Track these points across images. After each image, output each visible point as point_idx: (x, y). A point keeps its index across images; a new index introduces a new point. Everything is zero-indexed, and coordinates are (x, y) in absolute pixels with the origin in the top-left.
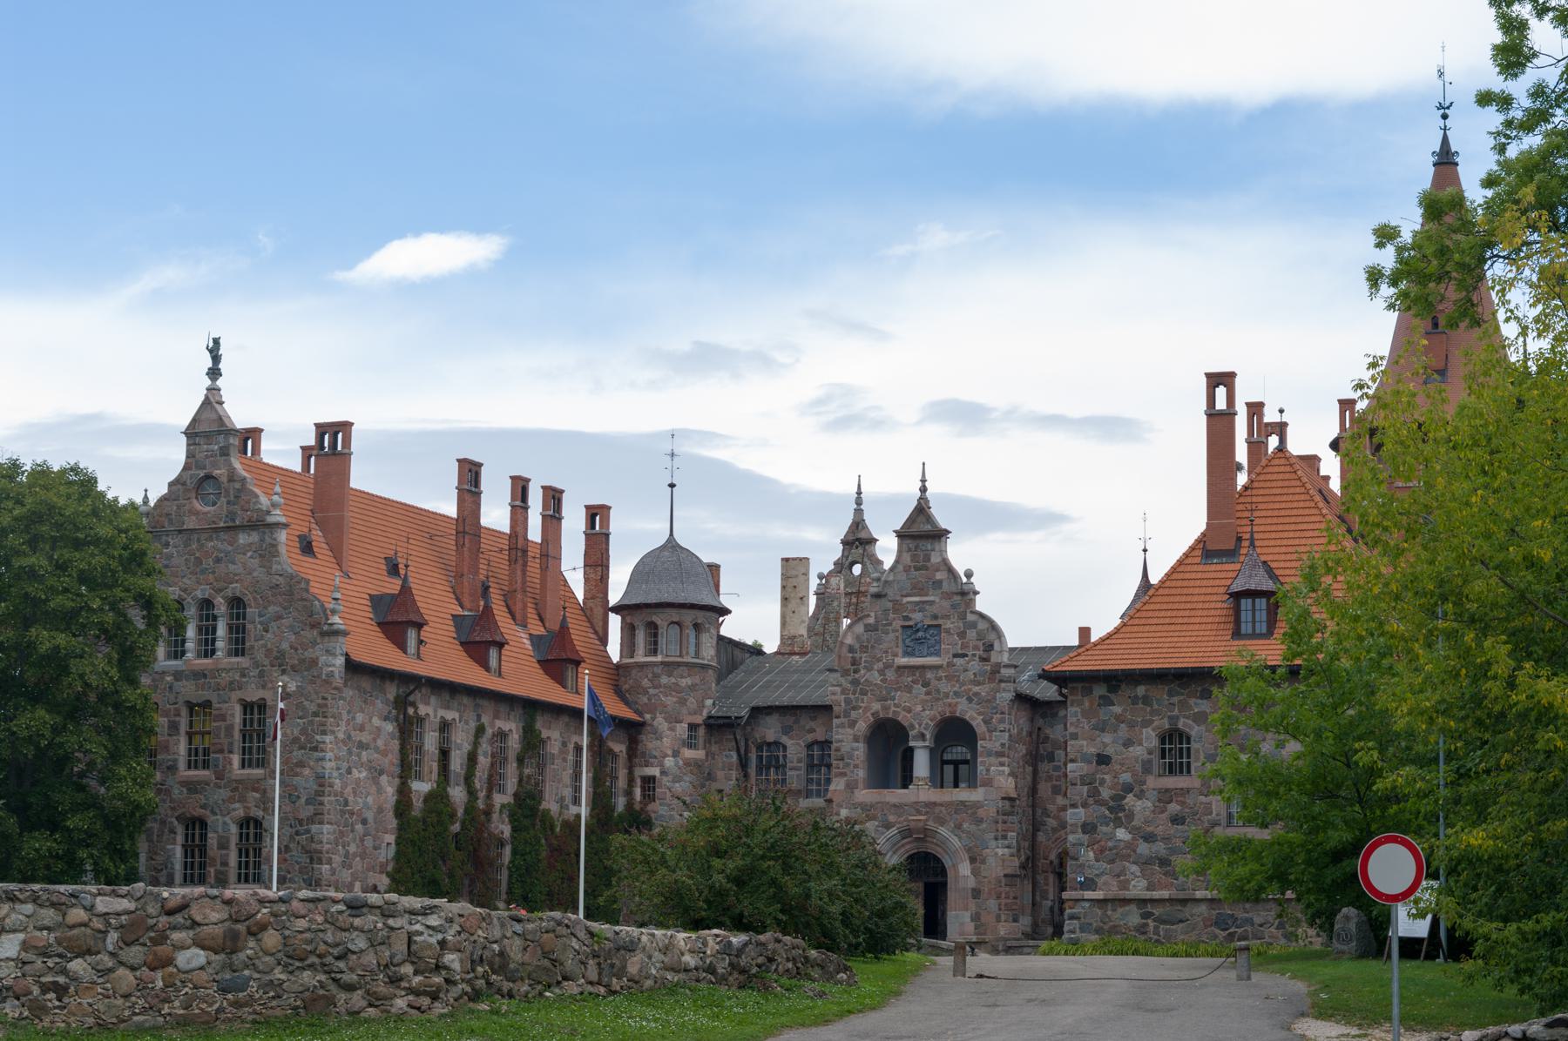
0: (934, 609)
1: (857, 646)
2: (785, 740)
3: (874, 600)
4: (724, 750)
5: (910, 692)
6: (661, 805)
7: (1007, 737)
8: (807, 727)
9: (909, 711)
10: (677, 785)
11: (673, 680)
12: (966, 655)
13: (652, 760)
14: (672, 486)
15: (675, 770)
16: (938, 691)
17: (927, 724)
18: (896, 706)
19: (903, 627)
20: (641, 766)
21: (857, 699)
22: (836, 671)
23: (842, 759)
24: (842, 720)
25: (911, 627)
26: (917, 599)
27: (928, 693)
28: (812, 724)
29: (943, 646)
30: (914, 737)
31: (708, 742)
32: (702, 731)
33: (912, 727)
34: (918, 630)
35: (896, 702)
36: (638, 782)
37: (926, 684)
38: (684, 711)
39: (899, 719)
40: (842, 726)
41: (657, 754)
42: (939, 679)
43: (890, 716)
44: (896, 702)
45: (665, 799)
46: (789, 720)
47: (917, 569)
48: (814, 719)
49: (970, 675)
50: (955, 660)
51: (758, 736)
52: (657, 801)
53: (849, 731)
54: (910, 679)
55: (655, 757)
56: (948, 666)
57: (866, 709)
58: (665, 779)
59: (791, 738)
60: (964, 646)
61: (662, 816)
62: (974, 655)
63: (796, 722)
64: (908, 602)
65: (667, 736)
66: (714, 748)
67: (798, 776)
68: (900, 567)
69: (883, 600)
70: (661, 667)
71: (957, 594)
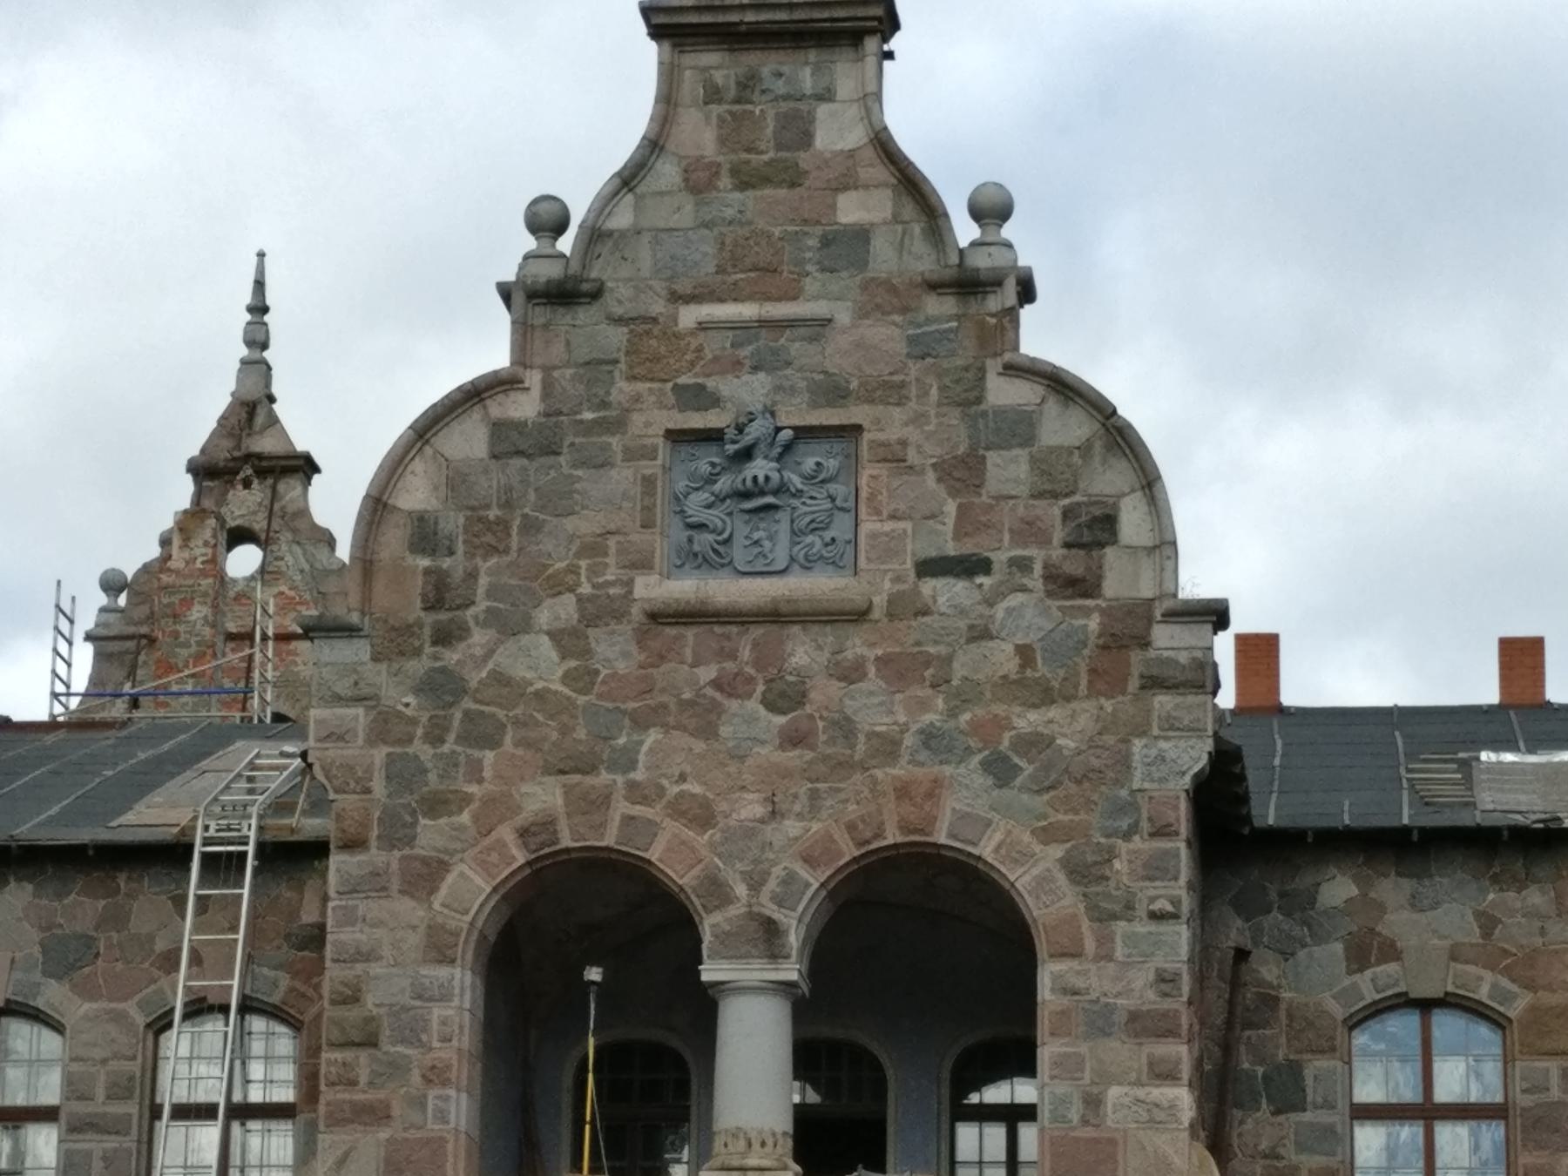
0: (836, 356)
3: (540, 315)
5: (708, 731)
7: (1184, 951)
9: (701, 816)
12: (982, 566)
16: (845, 728)
17: (789, 879)
18: (636, 792)
19: (677, 437)
21: (451, 761)
22: (348, 631)
23: (371, 1042)
24: (377, 855)
25: (712, 436)
26: (747, 311)
27: (794, 739)
29: (867, 527)
30: (722, 937)
33: (718, 892)
34: (746, 454)
35: (639, 775)
37: (785, 697)
39: (654, 855)
40: (375, 884)
42: (850, 674)
43: (609, 840)
44: (639, 775)
47: (746, 180)
49: (1002, 657)
50: (929, 586)
53: (406, 907)
54: (707, 673)
56: (891, 616)
57: (496, 808)
60: (966, 523)
62: (1022, 565)
64: (703, 327)
68: (667, 172)
69: (585, 315)
71: (934, 286)
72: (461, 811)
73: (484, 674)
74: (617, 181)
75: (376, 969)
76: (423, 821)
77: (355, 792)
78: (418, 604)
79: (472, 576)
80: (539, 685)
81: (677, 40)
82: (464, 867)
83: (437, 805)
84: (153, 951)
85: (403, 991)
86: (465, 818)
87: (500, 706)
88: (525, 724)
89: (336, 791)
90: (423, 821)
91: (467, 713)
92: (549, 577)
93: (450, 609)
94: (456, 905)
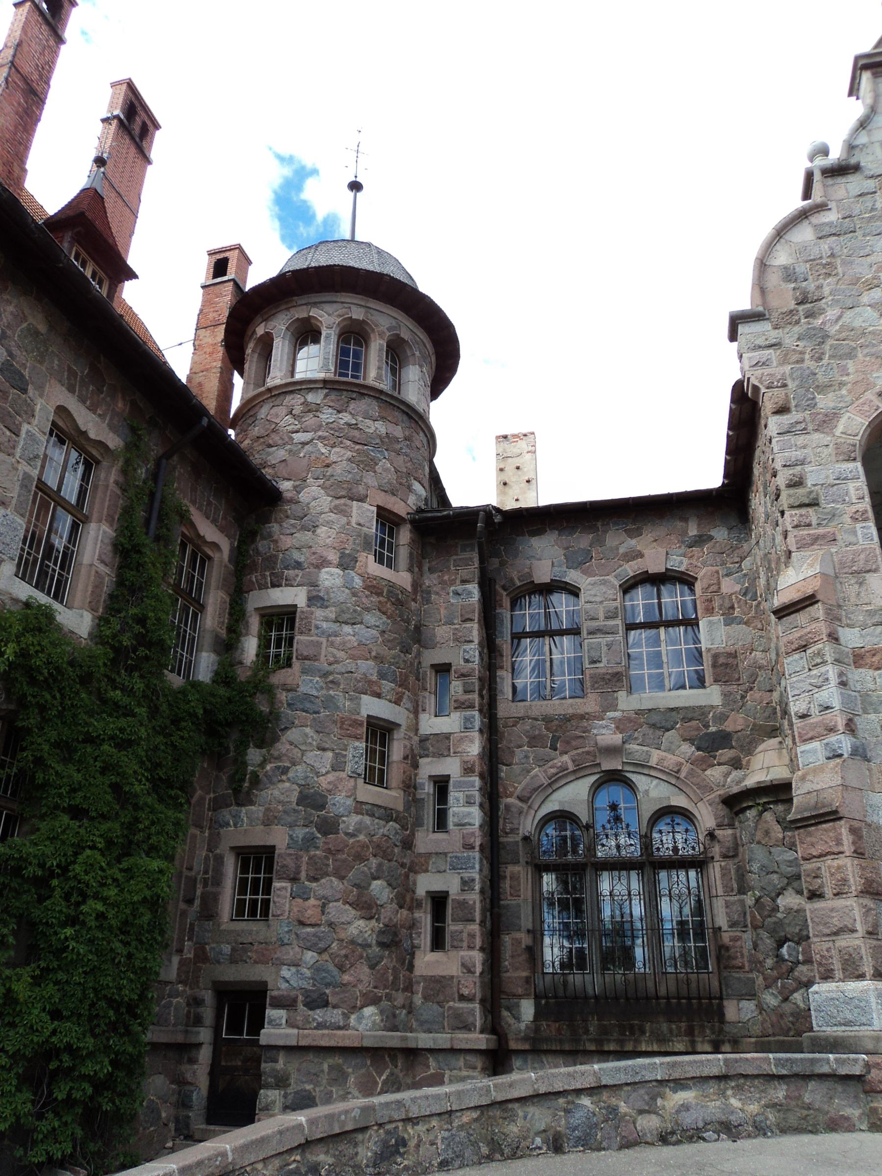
1: (802, 268)
2: (573, 577)
4: (452, 582)
6: (304, 671)
8: (622, 550)
10: (347, 629)
11: (346, 418)
13: (291, 573)
14: (355, 186)
15: (343, 595)
20: (263, 587)
23: (814, 504)
28: (632, 543)
31: (416, 565)
32: (405, 535)
36: (254, 623)
38: (370, 479)
41: (302, 559)
45: (315, 658)
46: (582, 540)
48: (635, 533)
51: (515, 575)
52: (296, 664)
55: (298, 565)
58: (319, 613)
59: (588, 573)
61: (307, 697)
63: (601, 542)
65: (329, 524)
66: (430, 580)
67: (609, 646)
70: (321, 394)
72: (840, 389)
73: (837, 327)
74: (858, 123)
75: (808, 468)
76: (818, 397)
77: (777, 387)
78: (793, 302)
79: (820, 287)
80: (871, 329)
81: (875, 70)
82: (848, 414)
83: (822, 389)
84: (618, 553)
85: (827, 477)
86: (844, 392)
87: (851, 340)
88: (867, 346)
89: (768, 388)
90: (818, 397)
91: (831, 346)
92: (863, 283)
93: (812, 302)
94: (849, 432)
